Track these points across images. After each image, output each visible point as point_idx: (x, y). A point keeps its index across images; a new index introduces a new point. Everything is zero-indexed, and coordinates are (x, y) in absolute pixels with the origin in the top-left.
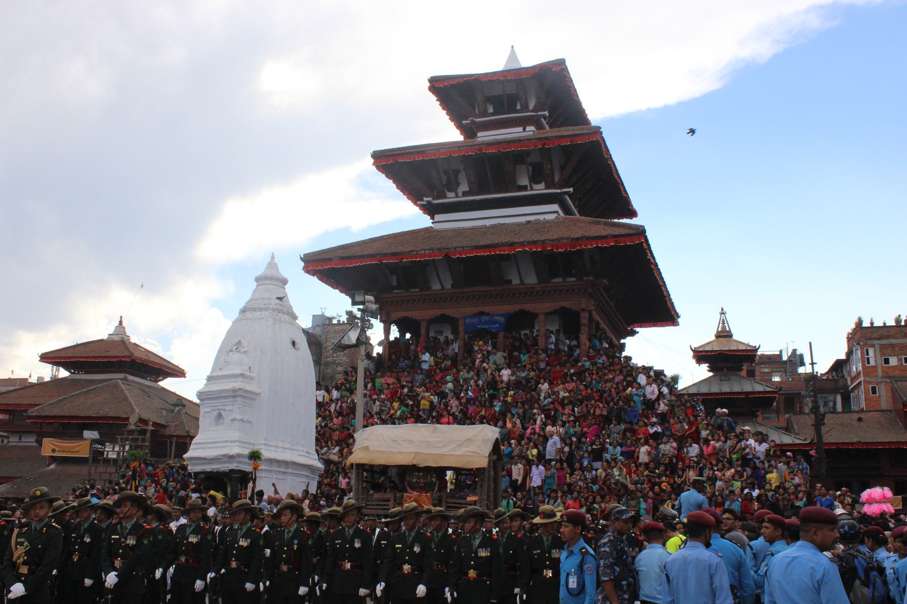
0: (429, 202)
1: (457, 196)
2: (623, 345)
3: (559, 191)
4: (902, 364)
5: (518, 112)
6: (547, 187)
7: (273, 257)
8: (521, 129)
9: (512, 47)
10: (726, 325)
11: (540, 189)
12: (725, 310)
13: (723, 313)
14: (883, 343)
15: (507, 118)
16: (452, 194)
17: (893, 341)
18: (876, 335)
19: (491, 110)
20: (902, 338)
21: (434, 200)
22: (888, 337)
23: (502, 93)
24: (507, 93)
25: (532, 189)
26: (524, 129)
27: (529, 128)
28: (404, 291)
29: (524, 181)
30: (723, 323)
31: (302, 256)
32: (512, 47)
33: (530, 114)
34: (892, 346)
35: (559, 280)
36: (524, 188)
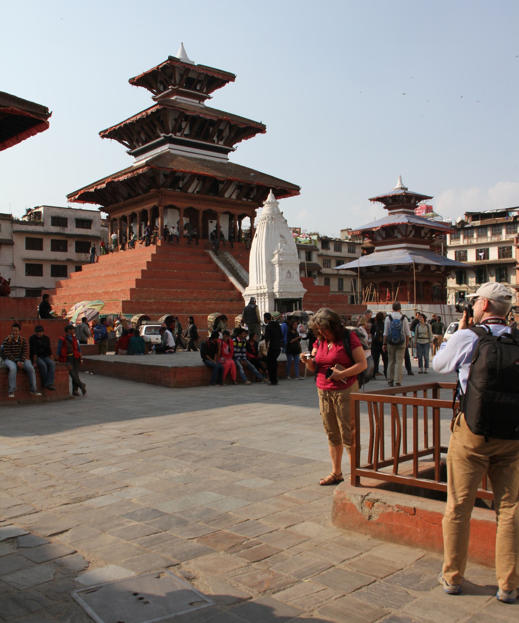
0: (171, 136)
1: (181, 136)
5: (198, 91)
6: (225, 144)
8: (197, 101)
9: (182, 43)
15: (193, 93)
19: (184, 85)
21: (172, 136)
23: (196, 78)
24: (199, 79)
25: (217, 143)
28: (172, 190)
29: (215, 139)
32: (182, 43)
33: (205, 95)
36: (214, 142)
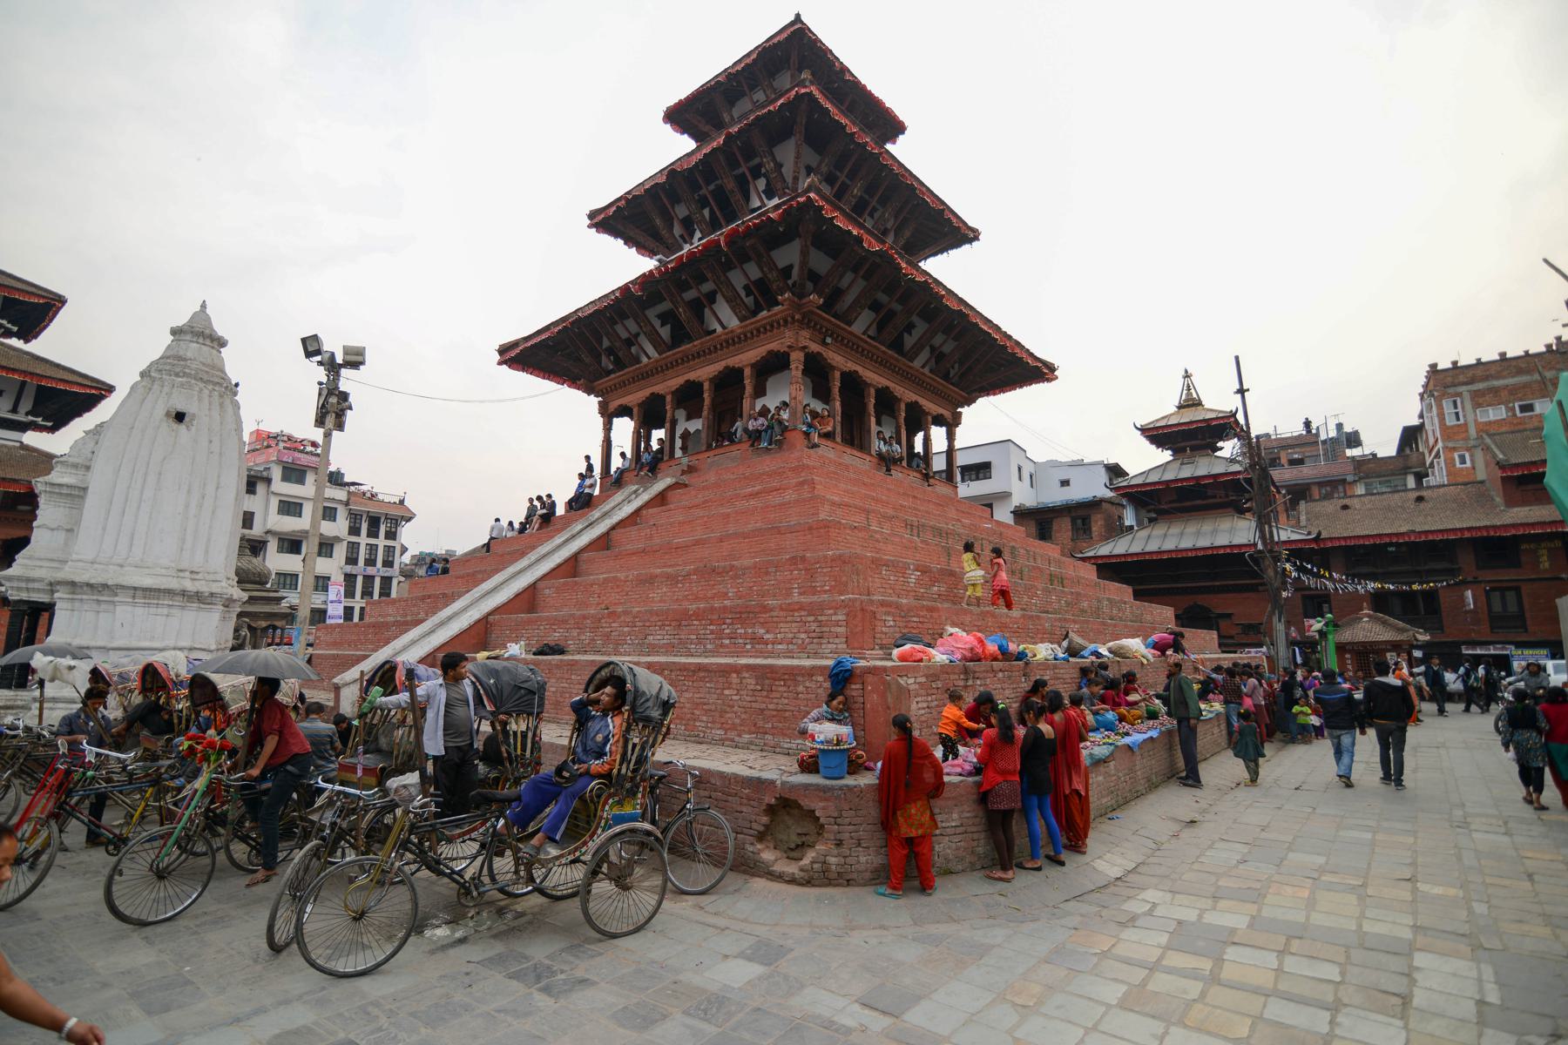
2: (960, 413)
4: (1515, 415)
10: (1193, 391)
13: (1187, 376)
14: (1475, 388)
17: (1496, 383)
18: (1462, 378)
20: (1513, 377)
22: (1486, 378)
30: (1189, 389)
34: (1495, 391)
35: (764, 313)
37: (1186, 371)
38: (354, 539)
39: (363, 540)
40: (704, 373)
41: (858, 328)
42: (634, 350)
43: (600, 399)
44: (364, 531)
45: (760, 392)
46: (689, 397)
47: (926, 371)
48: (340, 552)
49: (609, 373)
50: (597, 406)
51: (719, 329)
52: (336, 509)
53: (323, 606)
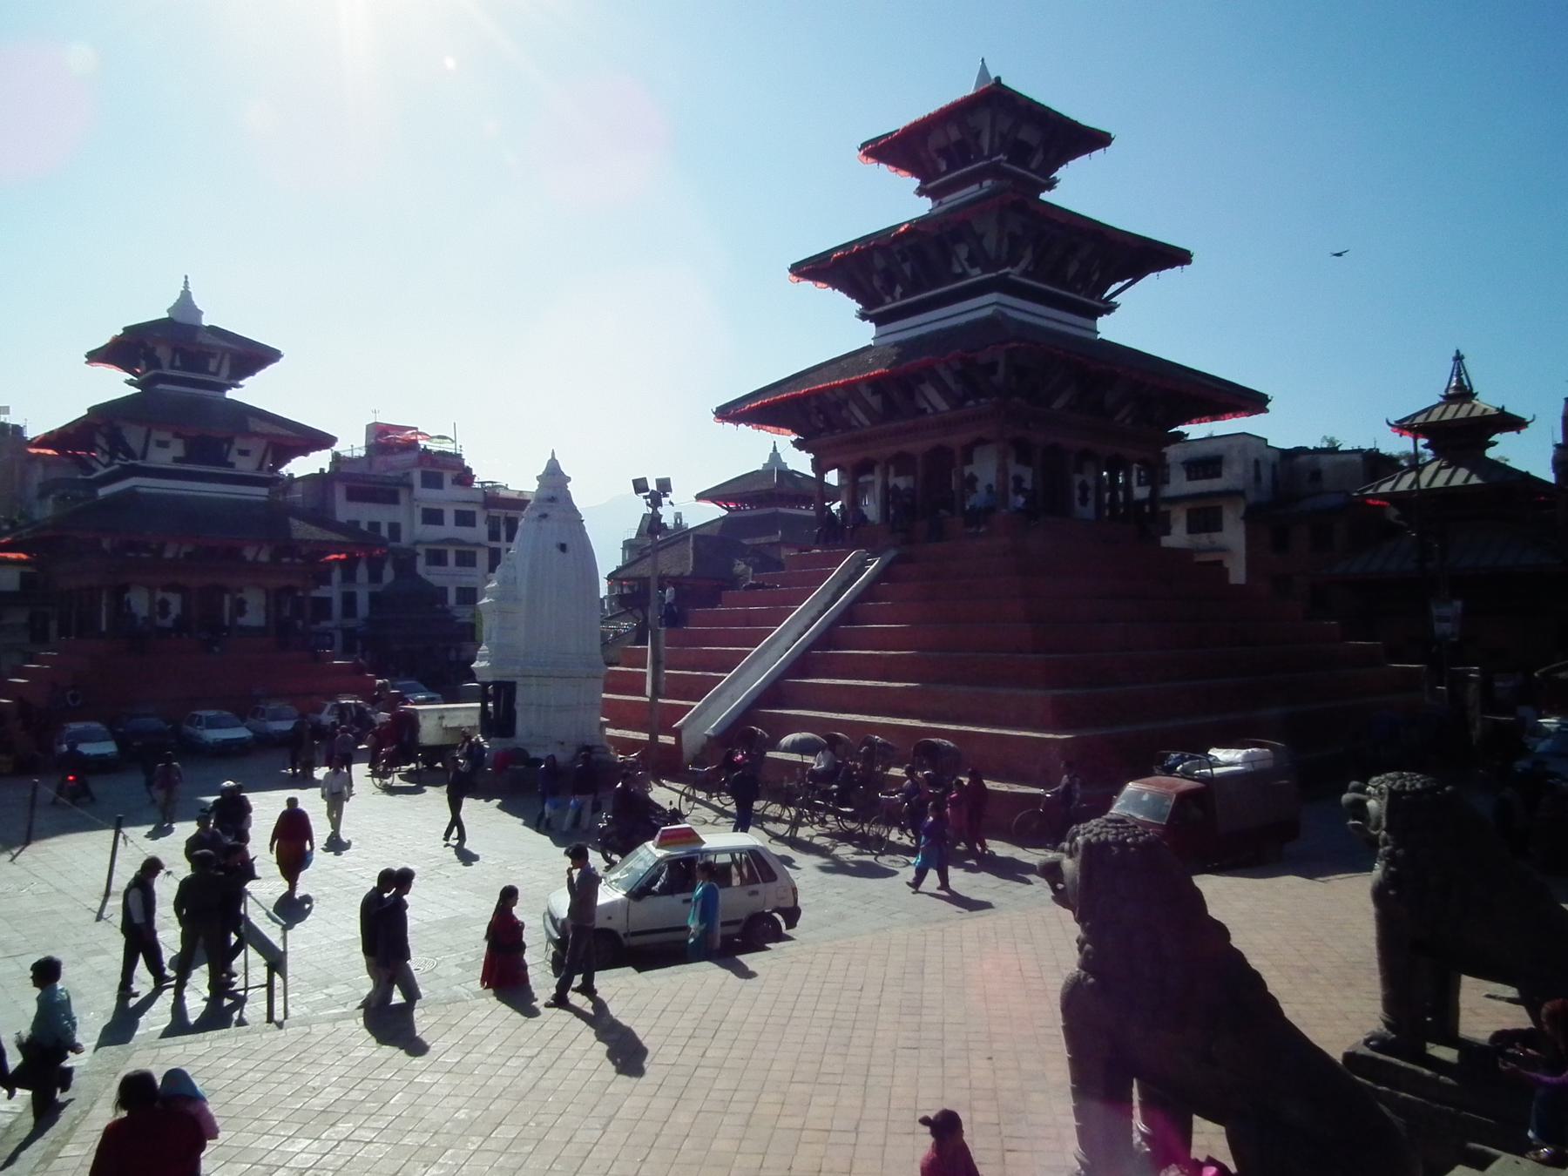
1: (894, 300)
2: (1165, 454)
3: (994, 275)
5: (970, 162)
6: (984, 272)
7: (553, 453)
10: (1463, 376)
11: (977, 275)
12: (1462, 353)
13: (1459, 358)
16: (888, 299)
19: (944, 167)
21: (870, 309)
26: (981, 186)
27: (987, 183)
30: (1459, 375)
31: (714, 410)
37: (1458, 352)
38: (494, 544)
39: (502, 544)
40: (916, 446)
41: (1058, 404)
42: (844, 413)
43: (811, 456)
44: (503, 535)
45: (969, 460)
46: (902, 462)
47: (1128, 421)
48: (483, 558)
49: (821, 430)
50: (810, 463)
51: (930, 410)
52: (473, 513)
53: (471, 620)
